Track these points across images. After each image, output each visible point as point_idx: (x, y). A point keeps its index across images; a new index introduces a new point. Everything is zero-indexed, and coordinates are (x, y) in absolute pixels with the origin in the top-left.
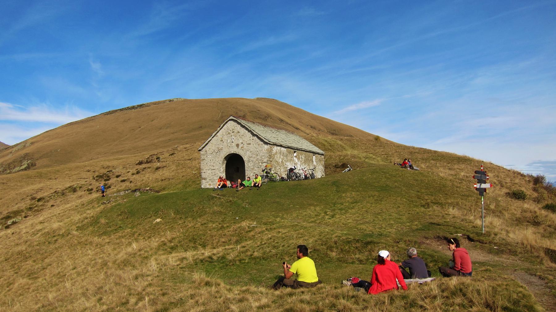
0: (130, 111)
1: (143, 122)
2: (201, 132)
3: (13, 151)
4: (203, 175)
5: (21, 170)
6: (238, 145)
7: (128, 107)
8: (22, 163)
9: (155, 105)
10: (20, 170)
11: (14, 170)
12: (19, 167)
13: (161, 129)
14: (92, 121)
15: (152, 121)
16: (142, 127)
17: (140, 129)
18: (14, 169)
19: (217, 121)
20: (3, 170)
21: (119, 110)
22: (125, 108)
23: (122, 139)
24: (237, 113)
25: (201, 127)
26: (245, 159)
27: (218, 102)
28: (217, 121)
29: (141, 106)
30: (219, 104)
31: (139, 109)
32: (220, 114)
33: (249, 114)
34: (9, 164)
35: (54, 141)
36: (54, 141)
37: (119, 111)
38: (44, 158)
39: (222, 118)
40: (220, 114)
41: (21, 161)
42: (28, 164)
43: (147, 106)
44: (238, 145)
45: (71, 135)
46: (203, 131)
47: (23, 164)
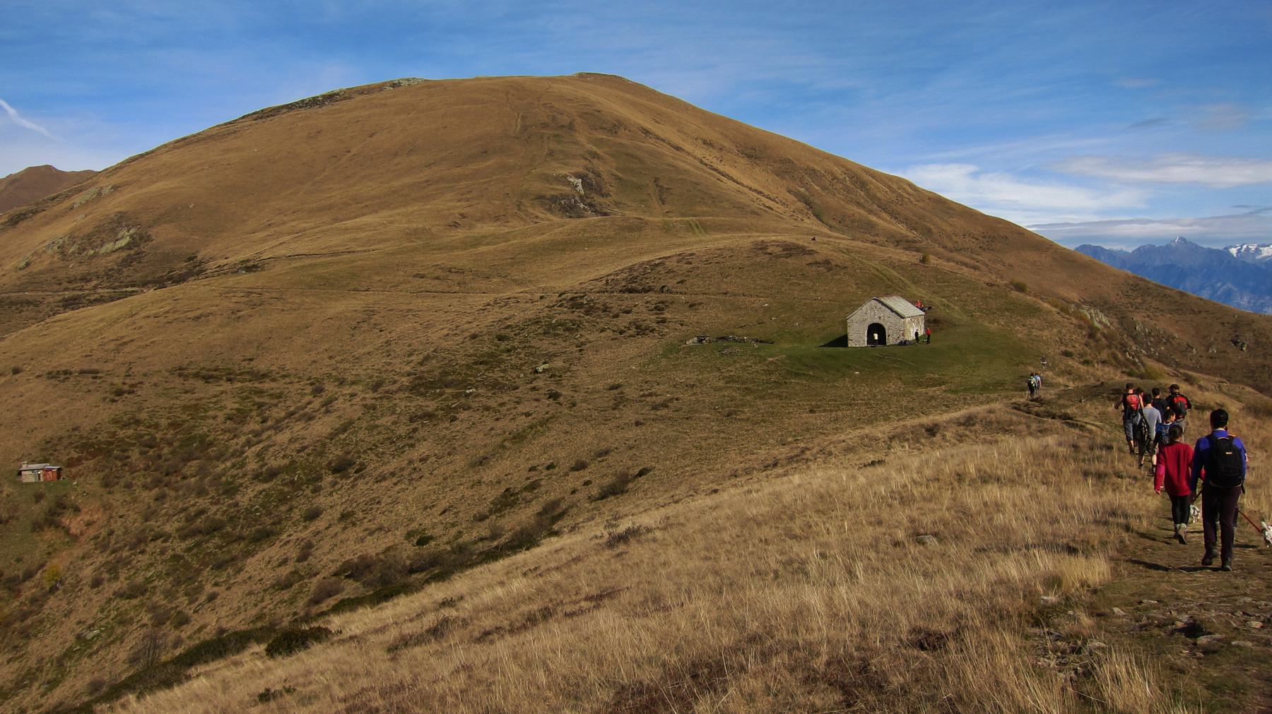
0: (316, 109)
1: (352, 138)
2: (488, 163)
3: (75, 206)
4: (850, 337)
5: (119, 248)
6: (880, 318)
7: (303, 101)
8: (116, 234)
9: (363, 97)
10: (116, 250)
11: (103, 250)
12: (112, 243)
13: (396, 155)
14: (233, 136)
15: (371, 136)
16: (354, 151)
17: (349, 155)
18: (102, 246)
19: (517, 138)
20: (79, 248)
21: (283, 107)
22: (297, 103)
23: (318, 178)
24: (554, 119)
25: (486, 152)
26: (886, 327)
27: (508, 93)
28: (517, 138)
29: (331, 97)
30: (510, 96)
31: (328, 107)
32: (519, 120)
33: (579, 120)
34: (88, 235)
35: (161, 185)
36: (161, 185)
37: (284, 110)
38: (165, 223)
39: (526, 130)
40: (519, 120)
41: (114, 231)
42: (131, 236)
43: (346, 98)
44: (880, 318)
45: (200, 168)
46: (492, 161)
47: (120, 236)
